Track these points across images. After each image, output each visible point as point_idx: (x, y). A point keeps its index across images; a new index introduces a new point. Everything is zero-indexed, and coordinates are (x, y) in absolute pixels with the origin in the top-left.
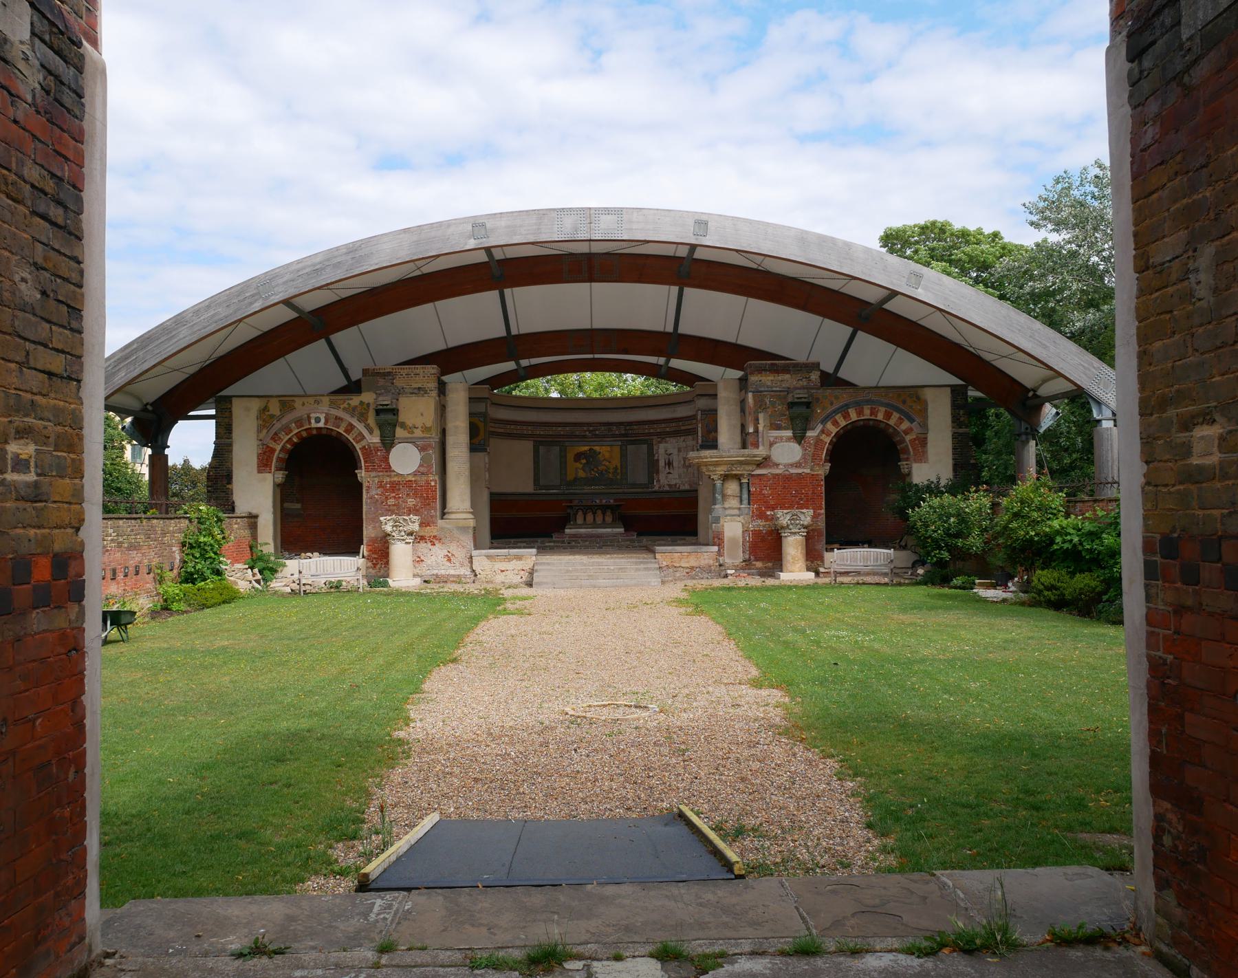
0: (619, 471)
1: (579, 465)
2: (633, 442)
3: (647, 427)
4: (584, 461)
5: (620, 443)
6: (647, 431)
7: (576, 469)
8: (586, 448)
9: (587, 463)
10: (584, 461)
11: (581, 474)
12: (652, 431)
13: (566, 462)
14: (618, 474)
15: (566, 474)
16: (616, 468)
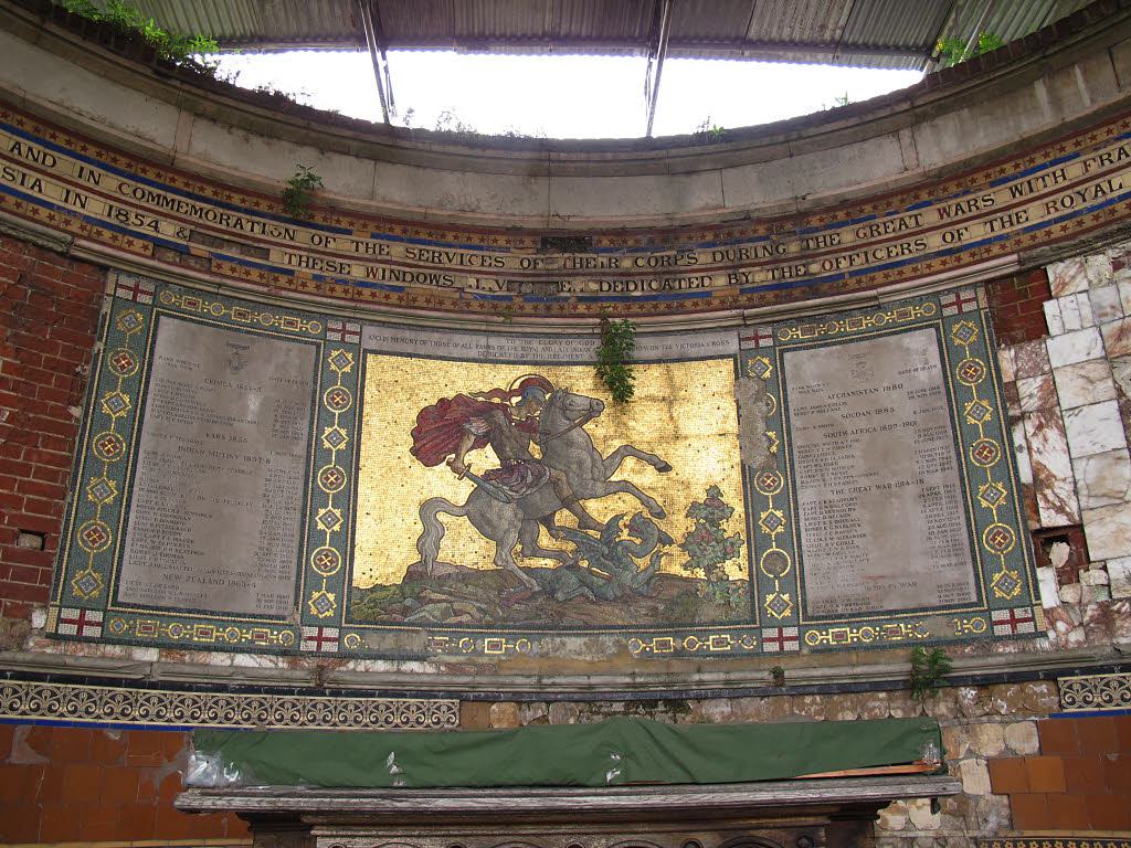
0: (733, 527)
1: (443, 482)
2: (822, 331)
3: (930, 217)
4: (484, 460)
5: (733, 347)
6: (935, 242)
7: (430, 509)
8: (504, 377)
9: (507, 469)
10: (484, 460)
11: (466, 548)
12: (976, 232)
13: (351, 460)
14: (729, 551)
15: (346, 541)
16: (711, 507)
